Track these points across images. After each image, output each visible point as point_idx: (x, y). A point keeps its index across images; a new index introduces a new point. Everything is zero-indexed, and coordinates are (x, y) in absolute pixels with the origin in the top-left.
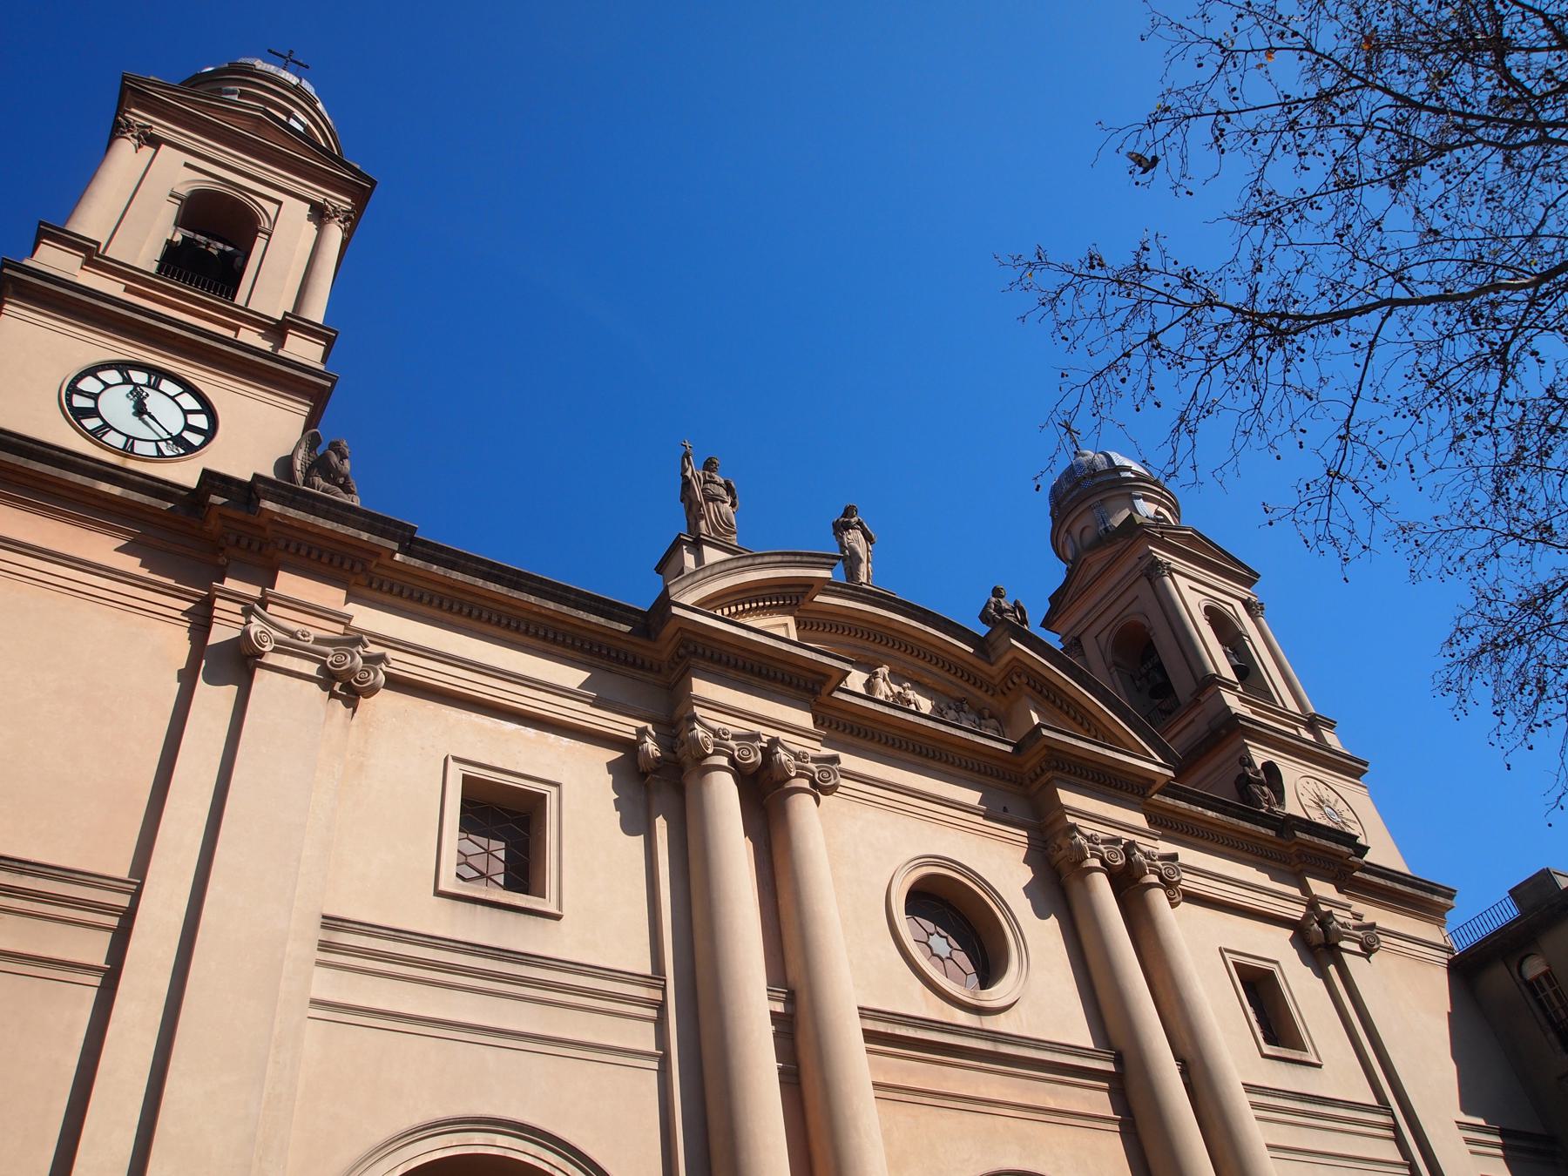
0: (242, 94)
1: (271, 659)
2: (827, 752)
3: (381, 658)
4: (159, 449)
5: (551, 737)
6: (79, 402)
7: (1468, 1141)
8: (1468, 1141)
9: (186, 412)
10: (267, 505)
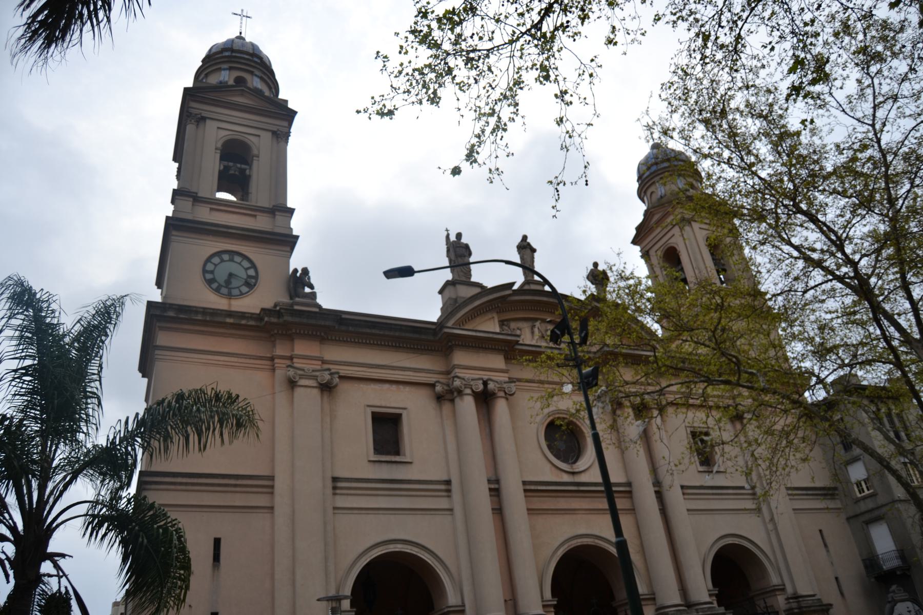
5: (401, 387)
6: (209, 276)
7: (789, 495)
8: (789, 495)
9: (246, 269)
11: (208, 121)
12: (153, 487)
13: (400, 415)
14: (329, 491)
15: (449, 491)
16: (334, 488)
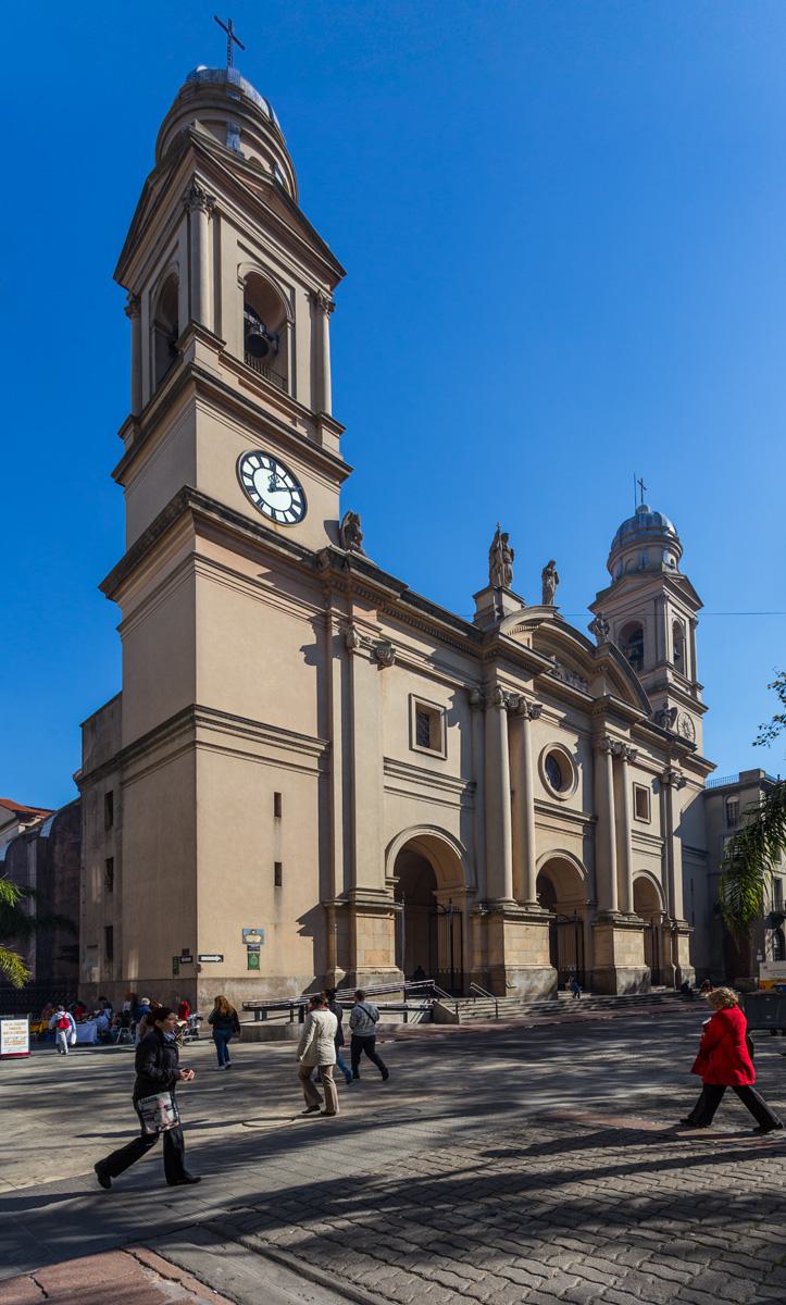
2: (539, 703)
10: (353, 570)
14: (381, 770)
16: (385, 768)
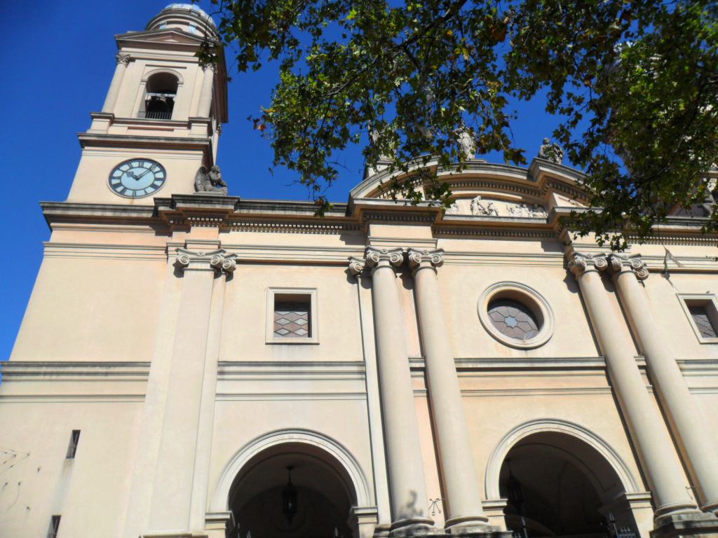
0: (169, 23)
1: (191, 266)
3: (234, 255)
4: (146, 192)
6: (114, 182)
11: (136, 61)
12: (14, 377)
13: (309, 296)
15: (365, 373)
